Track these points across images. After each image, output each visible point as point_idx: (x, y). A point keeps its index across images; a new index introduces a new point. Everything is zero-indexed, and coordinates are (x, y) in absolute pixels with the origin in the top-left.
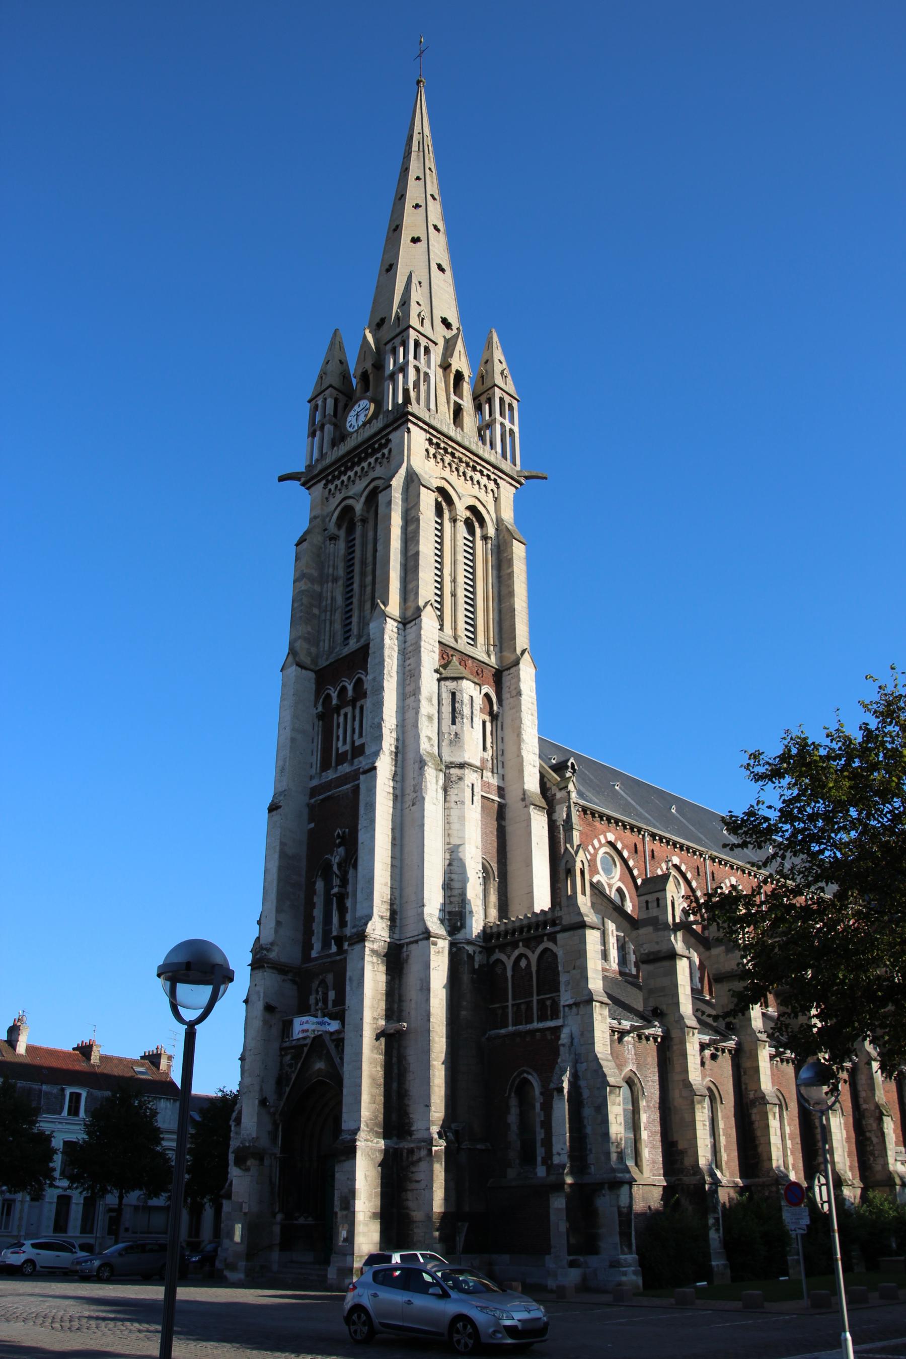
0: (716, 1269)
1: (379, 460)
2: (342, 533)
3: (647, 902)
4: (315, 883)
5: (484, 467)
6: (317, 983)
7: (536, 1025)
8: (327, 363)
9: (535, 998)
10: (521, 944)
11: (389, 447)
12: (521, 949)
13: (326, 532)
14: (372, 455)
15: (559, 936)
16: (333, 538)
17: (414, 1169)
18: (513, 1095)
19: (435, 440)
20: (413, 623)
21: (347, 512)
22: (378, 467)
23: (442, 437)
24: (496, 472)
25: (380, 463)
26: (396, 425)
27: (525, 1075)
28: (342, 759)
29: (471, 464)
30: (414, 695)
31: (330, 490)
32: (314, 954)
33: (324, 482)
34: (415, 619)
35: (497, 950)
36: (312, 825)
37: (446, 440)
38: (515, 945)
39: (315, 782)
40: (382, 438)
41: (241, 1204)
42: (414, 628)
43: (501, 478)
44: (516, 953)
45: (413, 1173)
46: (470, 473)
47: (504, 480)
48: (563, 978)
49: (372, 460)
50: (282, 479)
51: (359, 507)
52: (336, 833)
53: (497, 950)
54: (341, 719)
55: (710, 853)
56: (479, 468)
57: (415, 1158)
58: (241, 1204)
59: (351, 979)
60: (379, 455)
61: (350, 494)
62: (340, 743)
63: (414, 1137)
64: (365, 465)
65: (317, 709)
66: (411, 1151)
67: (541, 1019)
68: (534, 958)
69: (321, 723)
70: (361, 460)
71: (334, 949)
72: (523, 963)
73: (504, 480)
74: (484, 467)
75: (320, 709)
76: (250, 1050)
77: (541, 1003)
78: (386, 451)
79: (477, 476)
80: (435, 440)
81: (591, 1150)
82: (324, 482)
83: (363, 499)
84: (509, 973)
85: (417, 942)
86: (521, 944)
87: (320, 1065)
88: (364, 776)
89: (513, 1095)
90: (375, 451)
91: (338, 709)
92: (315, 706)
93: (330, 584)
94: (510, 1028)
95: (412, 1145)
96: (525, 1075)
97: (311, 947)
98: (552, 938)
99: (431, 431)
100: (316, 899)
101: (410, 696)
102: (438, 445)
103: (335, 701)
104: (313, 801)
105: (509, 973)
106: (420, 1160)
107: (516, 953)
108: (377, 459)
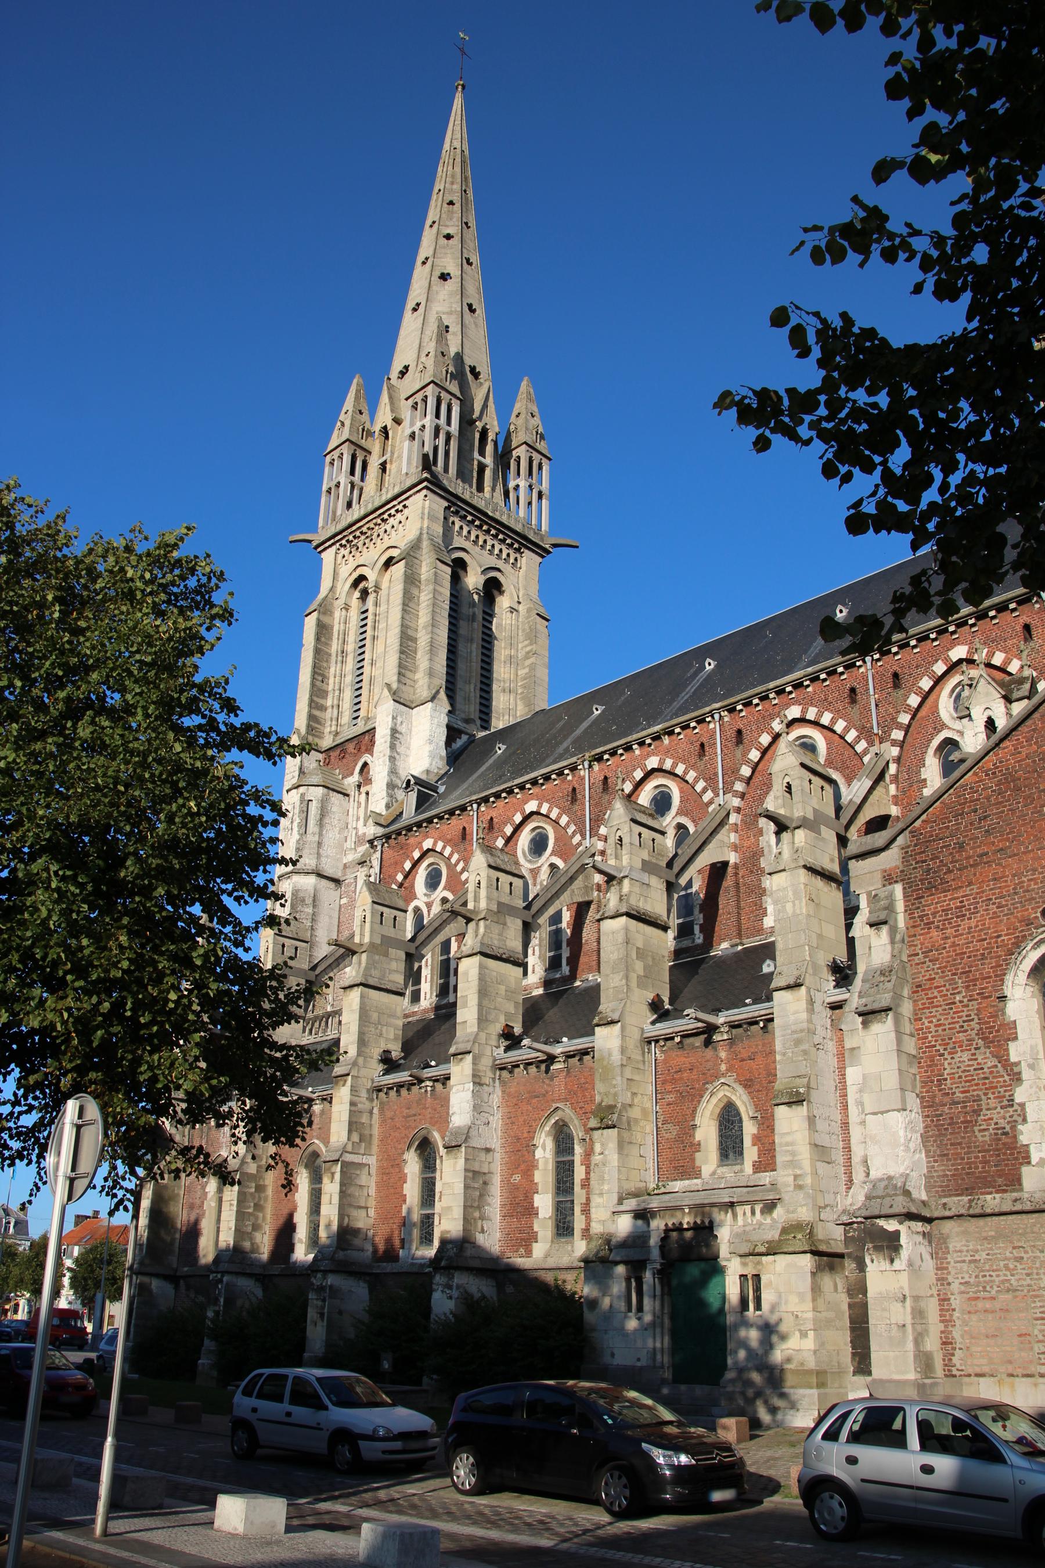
0: (200, 1368)
5: (394, 506)
19: (344, 542)
23: (345, 533)
24: (399, 500)
29: (379, 521)
37: (349, 531)
43: (407, 499)
46: (384, 527)
47: (410, 496)
55: (587, 755)
56: (385, 516)
73: (410, 496)
74: (394, 506)
79: (391, 521)
80: (344, 542)
99: (337, 538)
102: (348, 541)
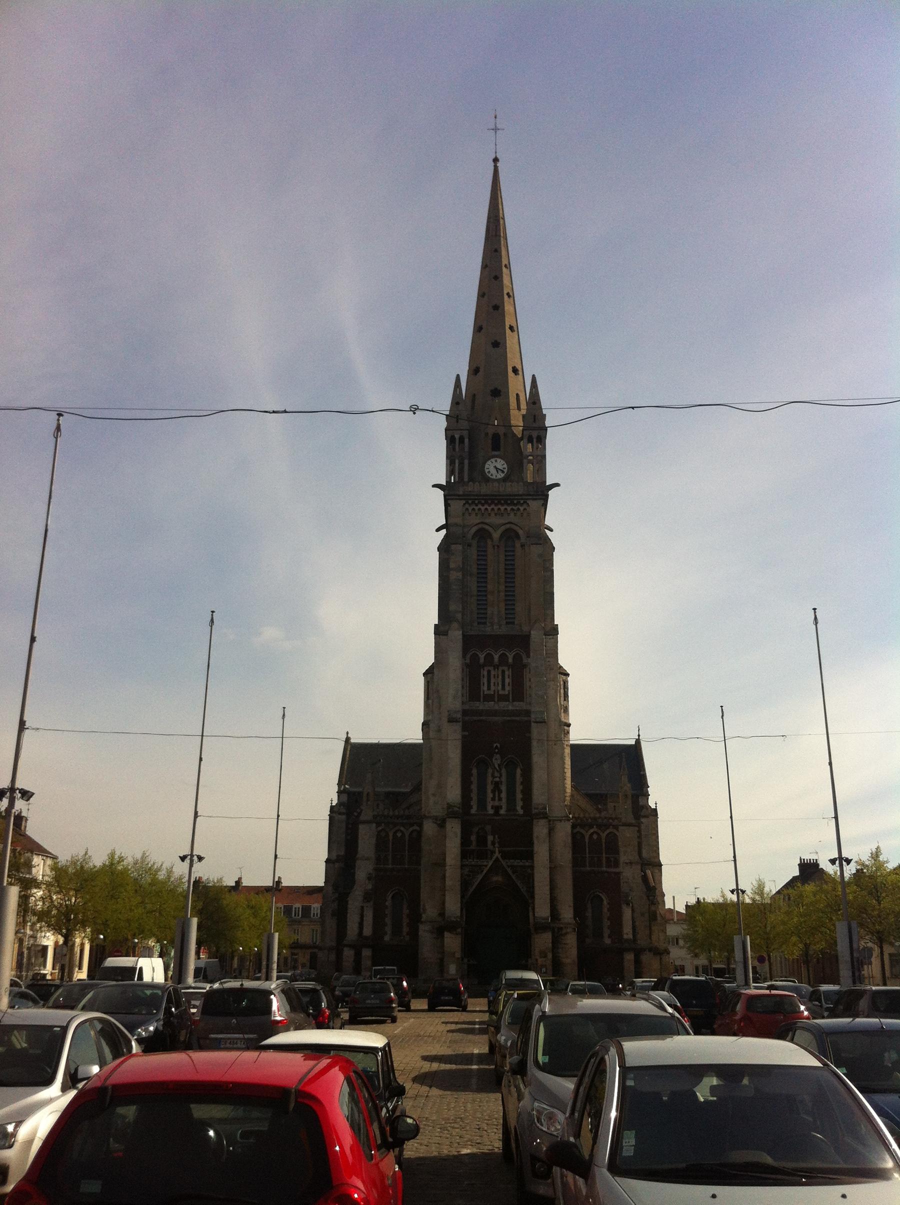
1: (515, 512)
2: (474, 543)
3: (615, 806)
4: (472, 769)
6: (477, 829)
7: (604, 869)
8: (458, 403)
9: (604, 855)
10: (595, 826)
11: (525, 506)
12: (595, 829)
13: (464, 539)
14: (508, 504)
15: (621, 828)
16: (469, 545)
17: (563, 938)
18: (589, 902)
20: (551, 637)
21: (482, 535)
22: (512, 515)
25: (515, 514)
26: (535, 497)
27: (598, 893)
28: (489, 698)
30: (553, 681)
31: (467, 509)
32: (473, 811)
33: (464, 502)
34: (554, 635)
35: (578, 827)
36: (467, 733)
38: (591, 827)
39: (467, 707)
40: (522, 499)
41: (454, 953)
42: (553, 640)
44: (592, 831)
45: (562, 939)
48: (622, 849)
49: (509, 508)
50: (434, 486)
51: (496, 535)
52: (495, 745)
53: (578, 827)
54: (486, 673)
57: (564, 931)
58: (454, 953)
59: (537, 837)
60: (515, 508)
61: (487, 521)
62: (485, 688)
63: (561, 921)
64: (502, 508)
65: (465, 660)
66: (562, 928)
67: (609, 866)
68: (604, 835)
69: (468, 669)
70: (499, 503)
71: (491, 811)
72: (595, 837)
75: (468, 661)
76: (451, 866)
77: (607, 858)
78: (522, 508)
81: (638, 933)
82: (464, 502)
83: (499, 532)
84: (587, 840)
85: (561, 821)
86: (595, 826)
87: (497, 878)
88: (536, 724)
89: (589, 902)
90: (512, 504)
91: (484, 666)
92: (464, 656)
93: (469, 577)
94: (588, 869)
95: (562, 926)
96: (598, 893)
97: (471, 807)
98: (616, 827)
100: (472, 779)
101: (550, 681)
103: (482, 661)
104: (467, 718)
105: (587, 840)
106: (566, 934)
107: (592, 831)
108: (512, 509)
